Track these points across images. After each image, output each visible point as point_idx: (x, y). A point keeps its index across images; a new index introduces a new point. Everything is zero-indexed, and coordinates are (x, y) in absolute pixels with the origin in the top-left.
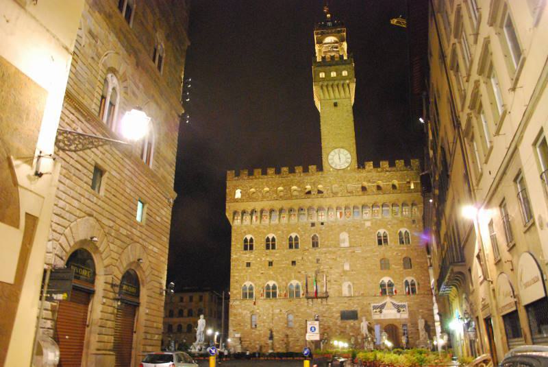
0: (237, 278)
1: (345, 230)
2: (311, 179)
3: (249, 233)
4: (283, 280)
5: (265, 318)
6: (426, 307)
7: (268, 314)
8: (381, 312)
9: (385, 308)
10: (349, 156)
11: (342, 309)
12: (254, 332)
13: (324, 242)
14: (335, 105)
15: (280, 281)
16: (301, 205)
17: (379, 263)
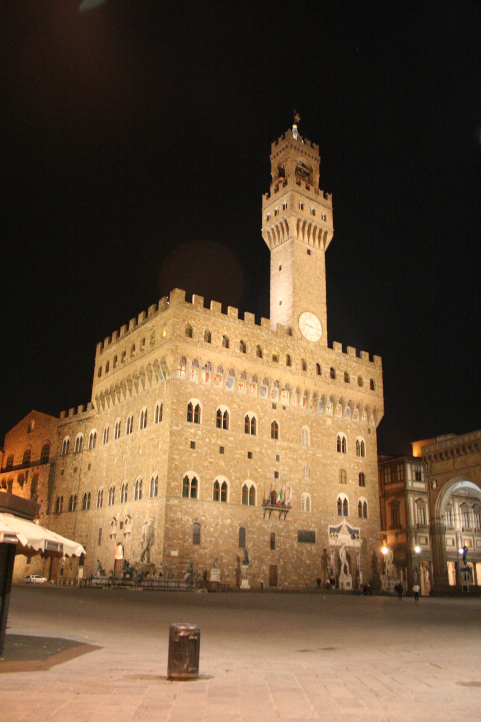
0: (177, 463)
1: (307, 424)
2: (280, 343)
3: (196, 396)
4: (236, 478)
5: (212, 530)
6: (375, 535)
7: (217, 525)
8: (337, 536)
9: (341, 532)
10: (320, 327)
11: (300, 528)
12: (198, 550)
13: (286, 433)
14: (309, 252)
15: (233, 478)
16: (267, 376)
17: (337, 474)
